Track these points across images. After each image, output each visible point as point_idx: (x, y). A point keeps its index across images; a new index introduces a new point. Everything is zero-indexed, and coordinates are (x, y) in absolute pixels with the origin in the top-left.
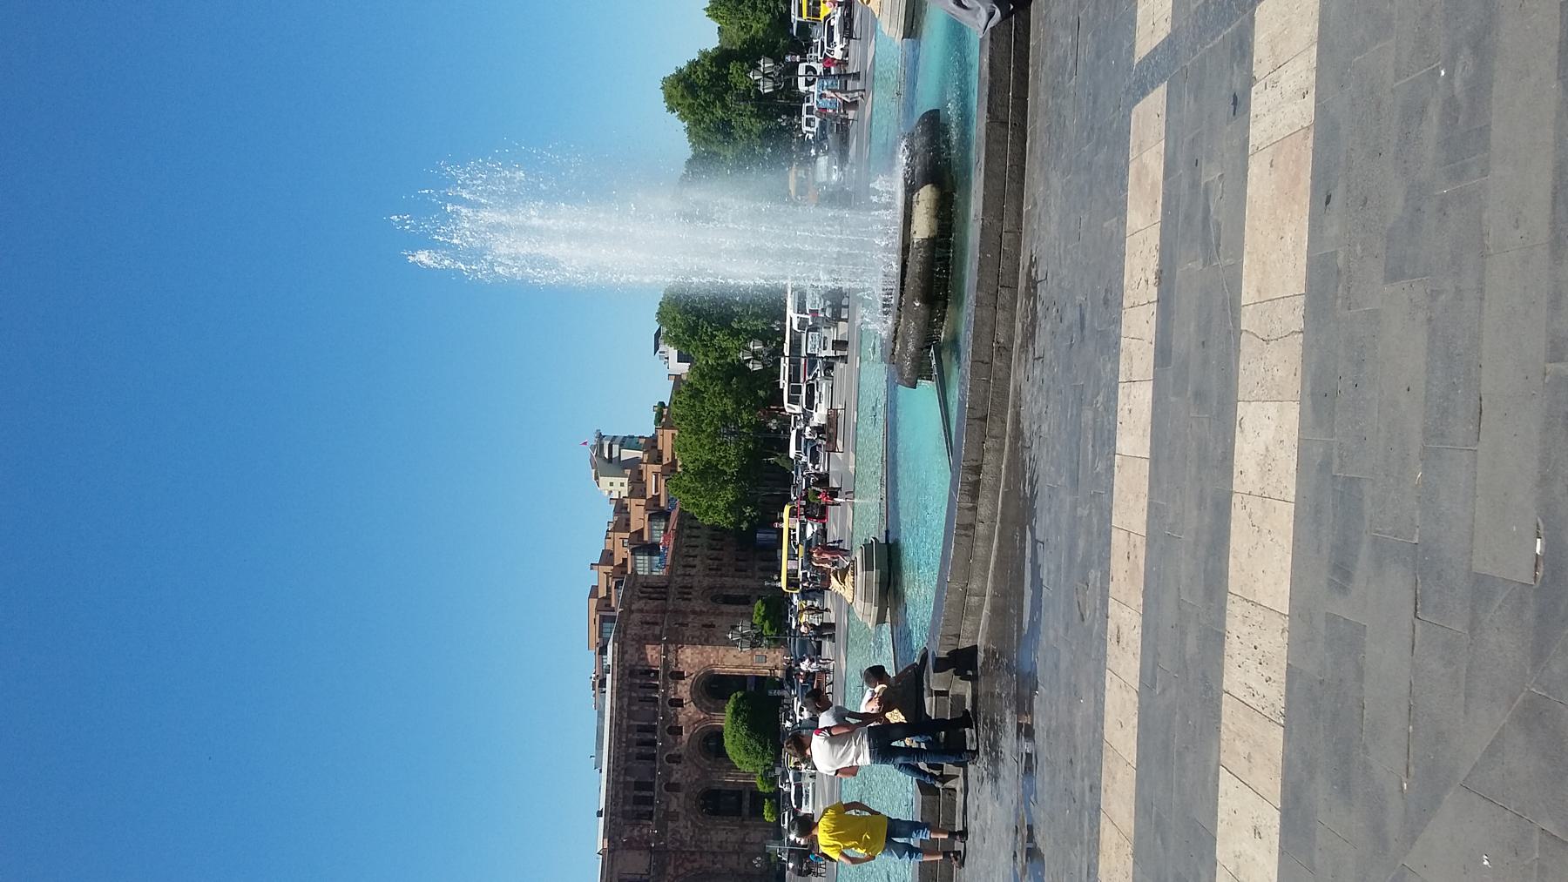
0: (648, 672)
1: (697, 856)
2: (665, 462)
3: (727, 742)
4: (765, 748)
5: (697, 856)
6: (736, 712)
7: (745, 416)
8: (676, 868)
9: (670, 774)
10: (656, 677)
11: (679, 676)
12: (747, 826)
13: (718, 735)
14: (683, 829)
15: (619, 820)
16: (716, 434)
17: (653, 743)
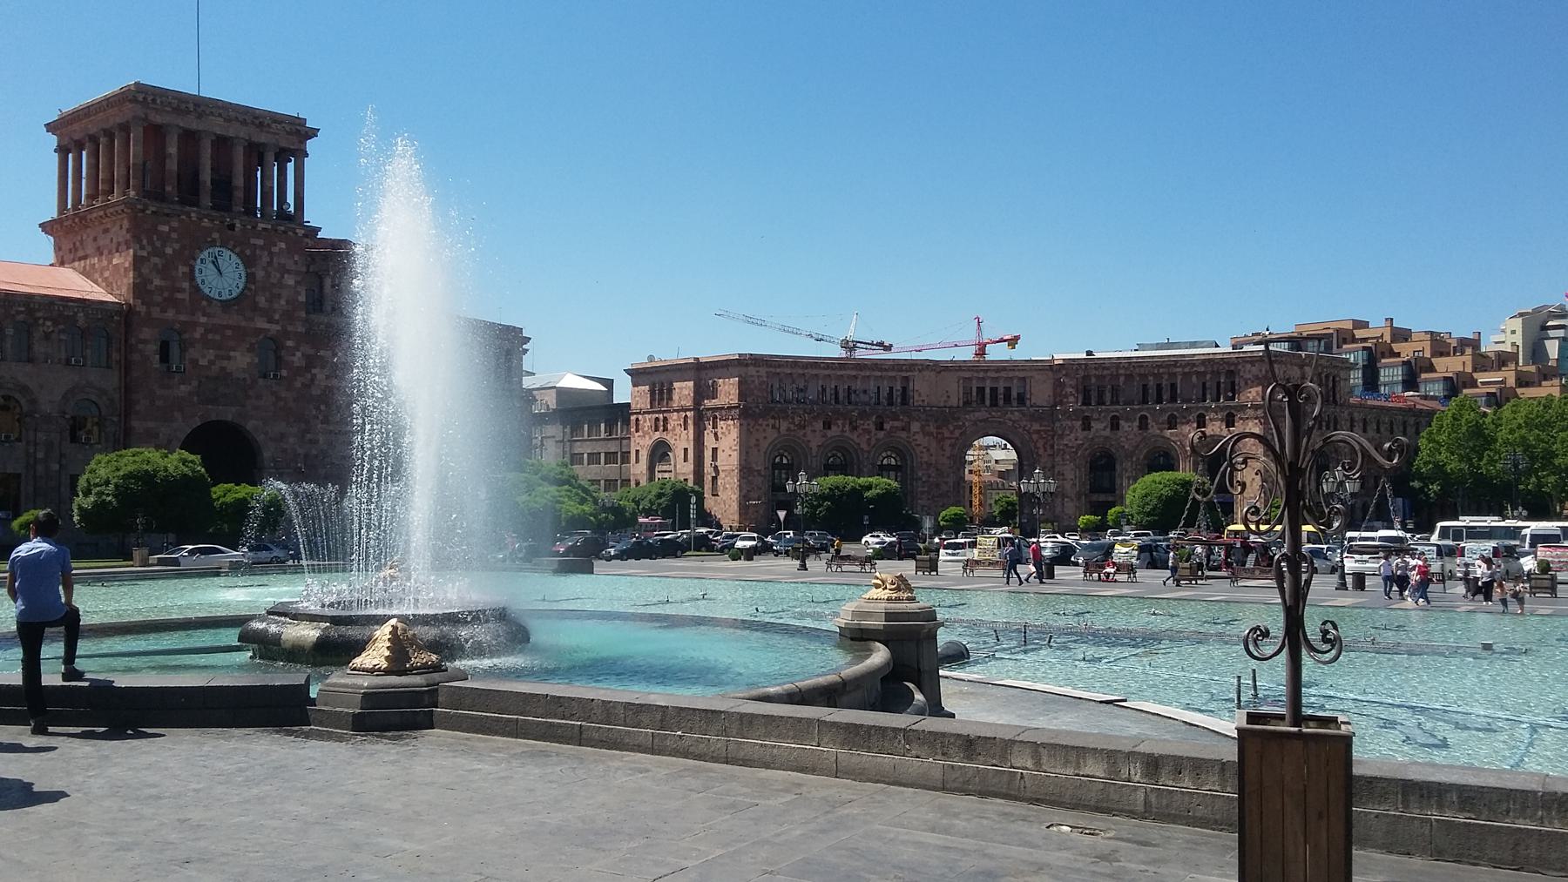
0: (1234, 390)
1: (1049, 452)
2: (1519, 391)
3: (1156, 476)
4: (1148, 514)
5: (1049, 452)
6: (1186, 484)
7: (1552, 479)
8: (1038, 432)
9: (1127, 420)
10: (1227, 399)
11: (1230, 422)
12: (1079, 499)
13: (1171, 467)
14: (1075, 436)
15: (1081, 373)
16: (1527, 448)
17: (1159, 401)
